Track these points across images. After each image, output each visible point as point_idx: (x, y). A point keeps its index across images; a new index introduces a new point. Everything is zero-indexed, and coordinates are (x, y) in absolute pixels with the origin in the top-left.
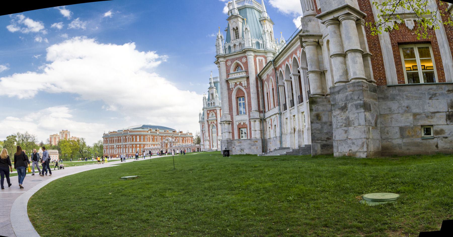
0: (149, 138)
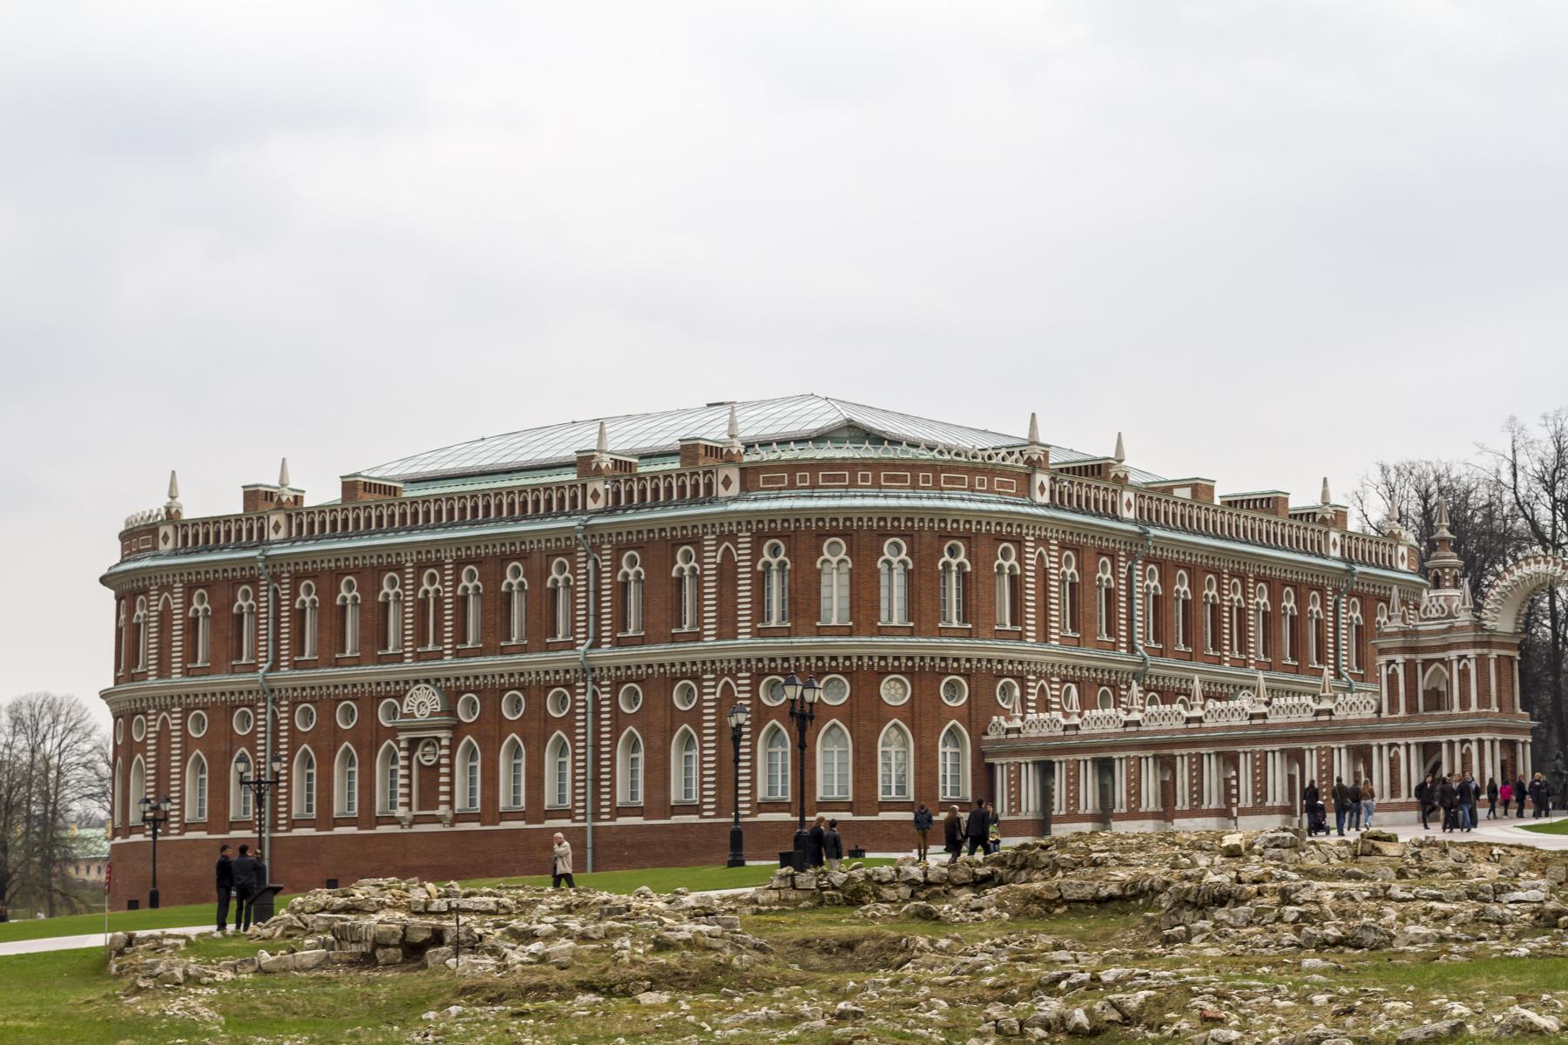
0: (1043, 574)
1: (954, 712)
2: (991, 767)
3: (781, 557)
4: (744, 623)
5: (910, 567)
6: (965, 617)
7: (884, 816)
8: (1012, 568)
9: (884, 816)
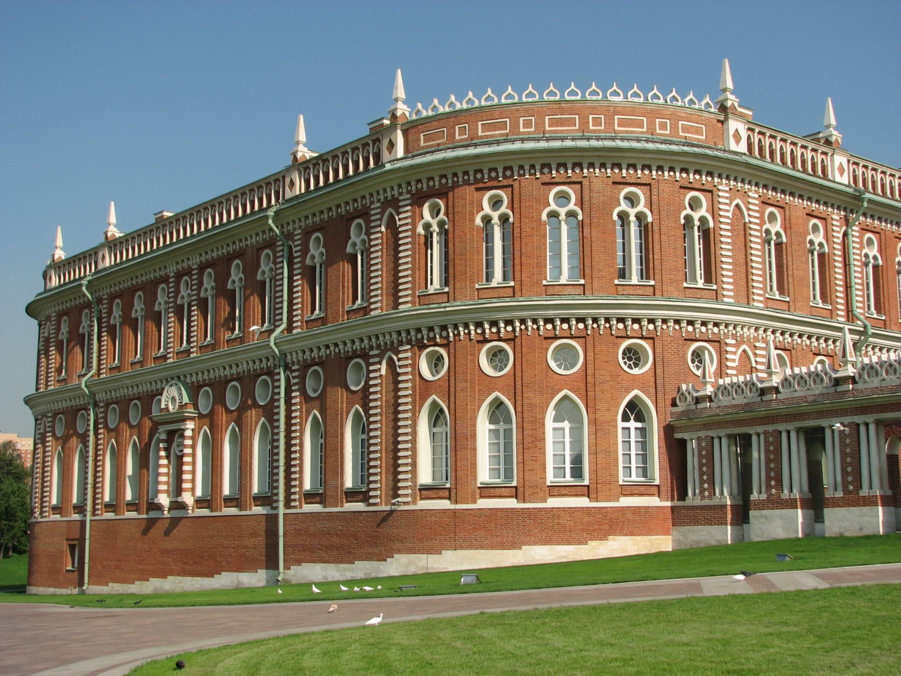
1: (636, 382)
2: (683, 443)
3: (442, 216)
4: (406, 295)
5: (580, 218)
6: (645, 274)
7: (553, 502)
8: (703, 220)
9: (553, 502)
